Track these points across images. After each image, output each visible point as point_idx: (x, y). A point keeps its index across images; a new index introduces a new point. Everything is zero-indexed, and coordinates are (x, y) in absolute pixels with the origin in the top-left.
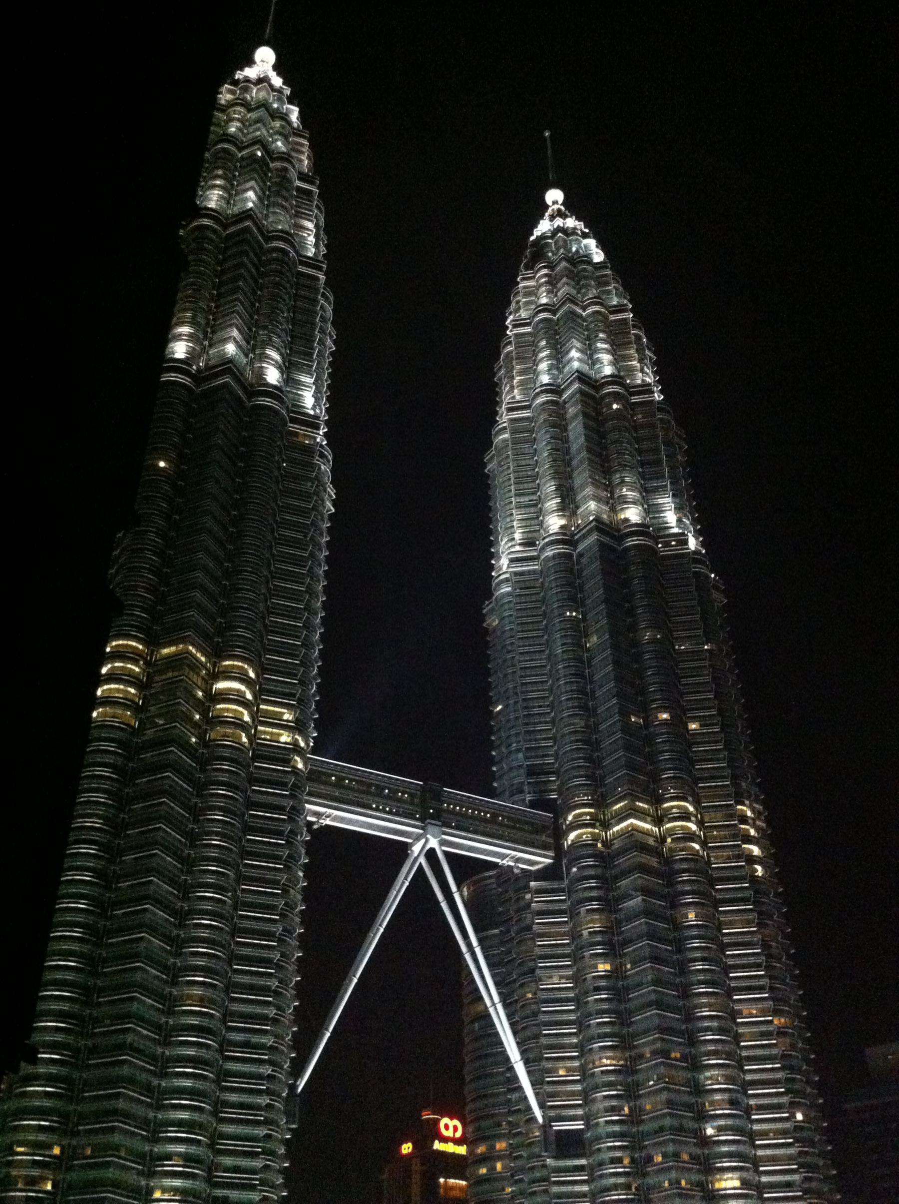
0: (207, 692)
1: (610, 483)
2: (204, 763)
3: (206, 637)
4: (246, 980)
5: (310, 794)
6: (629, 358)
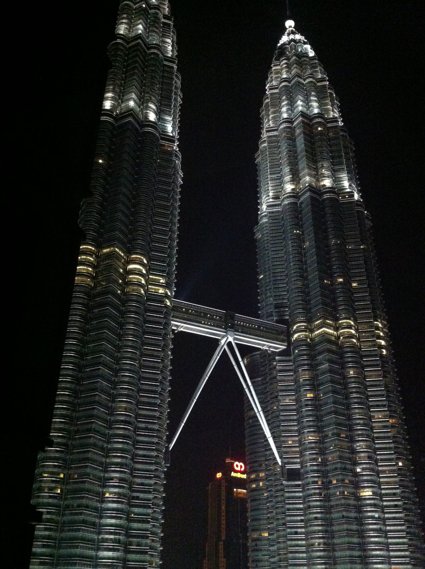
0: (125, 270)
1: (317, 167)
2: (124, 303)
3: (123, 243)
4: (146, 400)
5: (173, 317)
6: (326, 104)
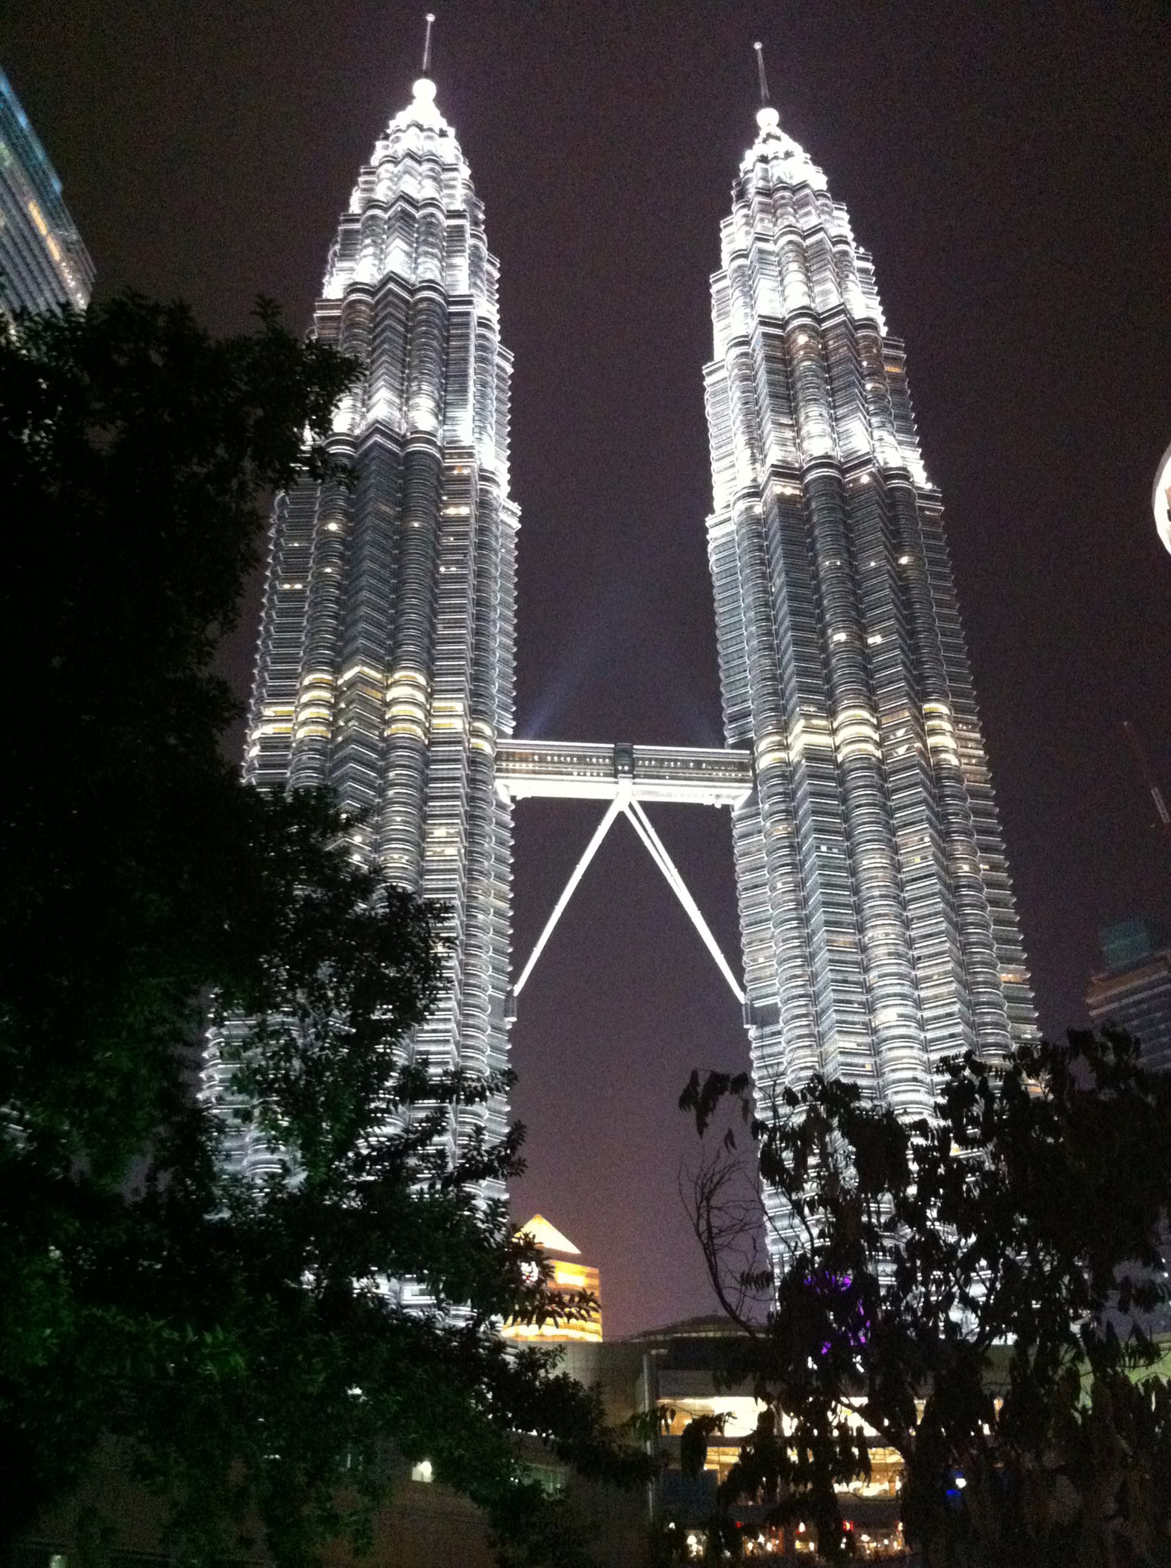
3: (379, 659)
5: (499, 770)
